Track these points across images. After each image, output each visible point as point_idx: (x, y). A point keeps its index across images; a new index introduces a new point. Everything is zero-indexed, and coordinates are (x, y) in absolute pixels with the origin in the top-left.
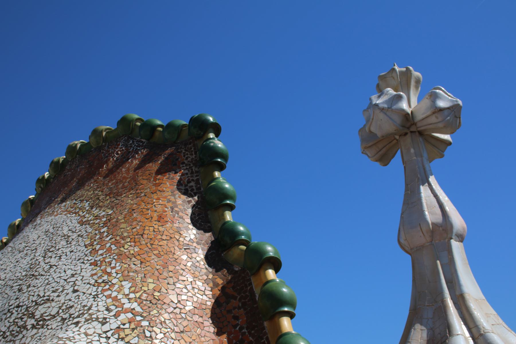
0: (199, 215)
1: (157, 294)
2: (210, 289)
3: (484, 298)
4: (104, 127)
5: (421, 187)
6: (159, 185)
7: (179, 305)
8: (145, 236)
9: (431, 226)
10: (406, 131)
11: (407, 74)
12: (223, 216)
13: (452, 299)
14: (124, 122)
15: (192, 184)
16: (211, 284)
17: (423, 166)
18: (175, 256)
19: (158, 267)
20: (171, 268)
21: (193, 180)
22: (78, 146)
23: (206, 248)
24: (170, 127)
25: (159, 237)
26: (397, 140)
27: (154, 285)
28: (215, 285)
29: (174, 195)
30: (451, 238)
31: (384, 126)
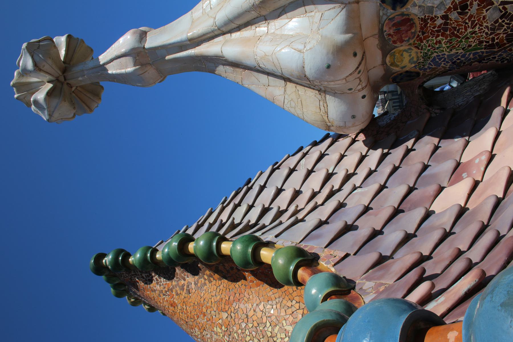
0: (165, 274)
1: (223, 328)
2: (215, 281)
3: (190, 12)
4: (128, 302)
5: (110, 72)
6: (151, 299)
7: (229, 312)
8: (187, 320)
9: (137, 67)
10: (65, 86)
11: (19, 86)
12: (161, 261)
13: (195, 47)
14: (119, 295)
15: (144, 275)
16: (212, 279)
17: (90, 69)
18: (196, 303)
19: (205, 320)
20: (204, 310)
21: (141, 275)
22: (147, 307)
23: (186, 273)
24: (108, 281)
25: (185, 310)
26: (77, 87)
27: (218, 328)
28: (211, 276)
29: (155, 291)
30: (144, 47)
31: (65, 109)
